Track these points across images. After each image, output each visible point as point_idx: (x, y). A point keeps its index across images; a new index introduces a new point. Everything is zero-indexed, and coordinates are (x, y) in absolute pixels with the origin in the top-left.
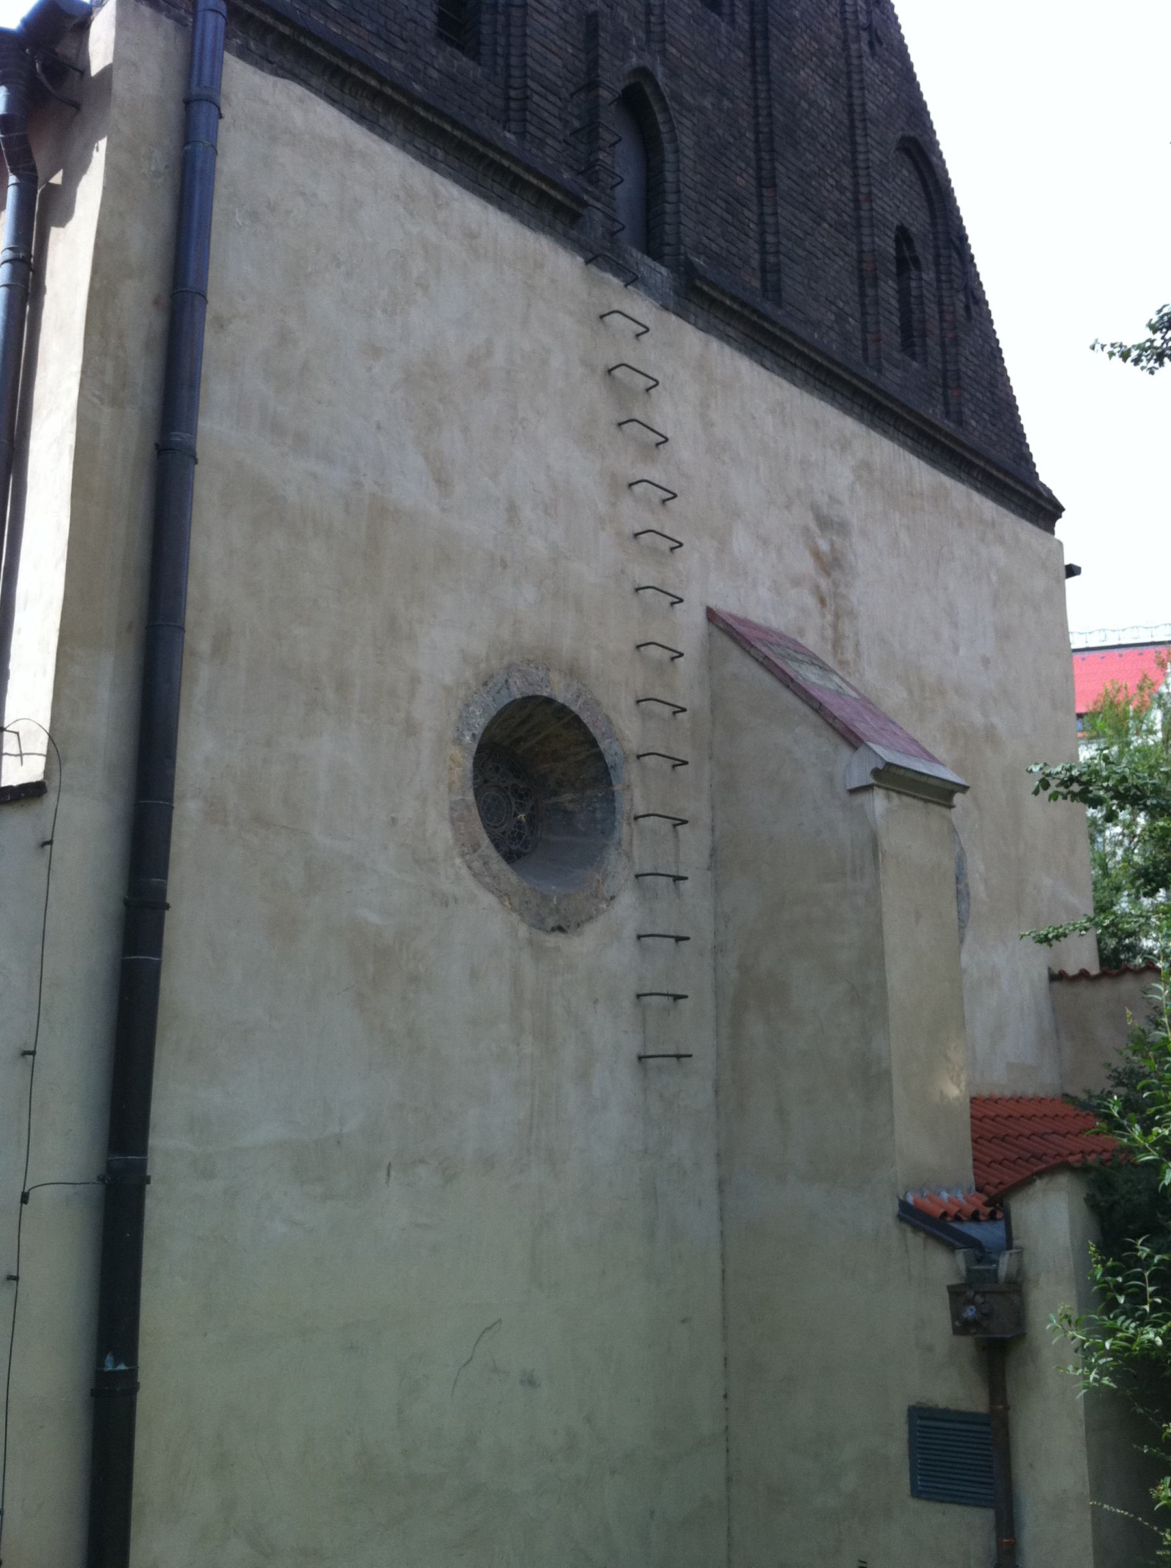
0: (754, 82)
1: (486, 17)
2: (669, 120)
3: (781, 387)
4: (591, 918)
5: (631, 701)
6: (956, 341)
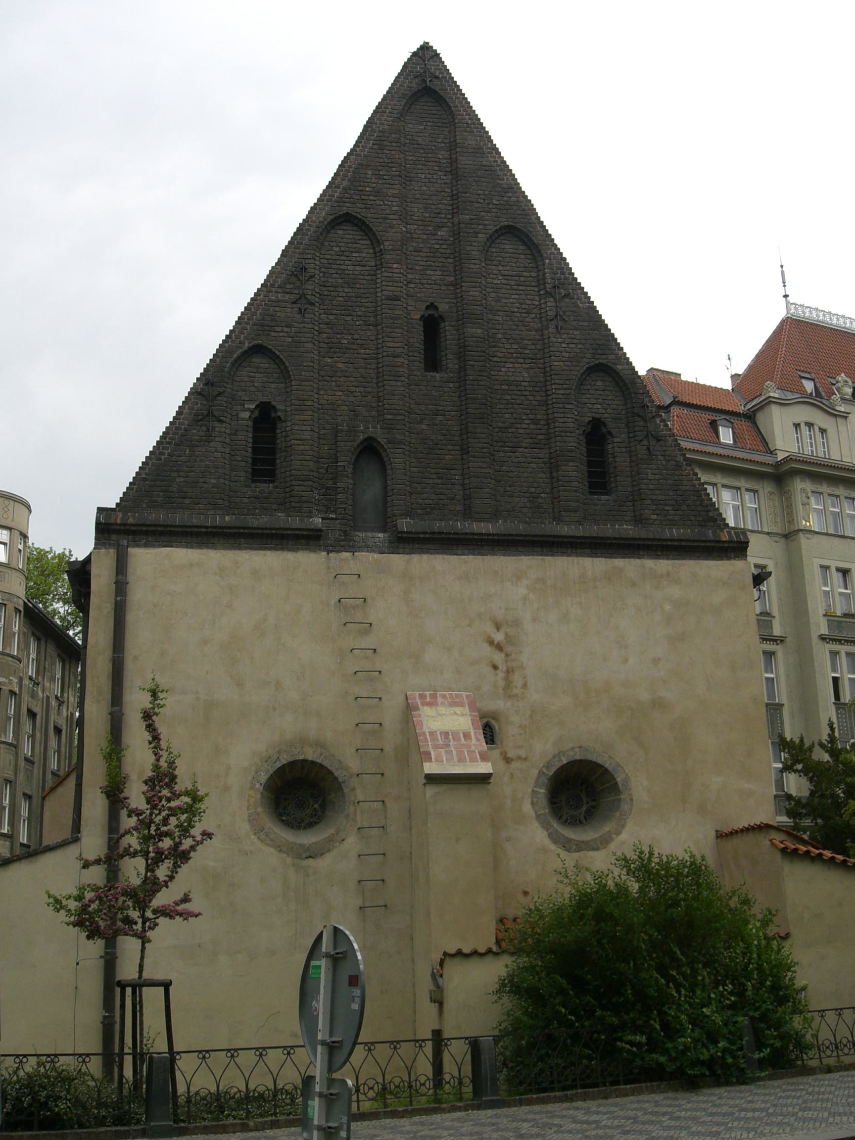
3: (466, 562)
4: (329, 851)
5: (354, 751)
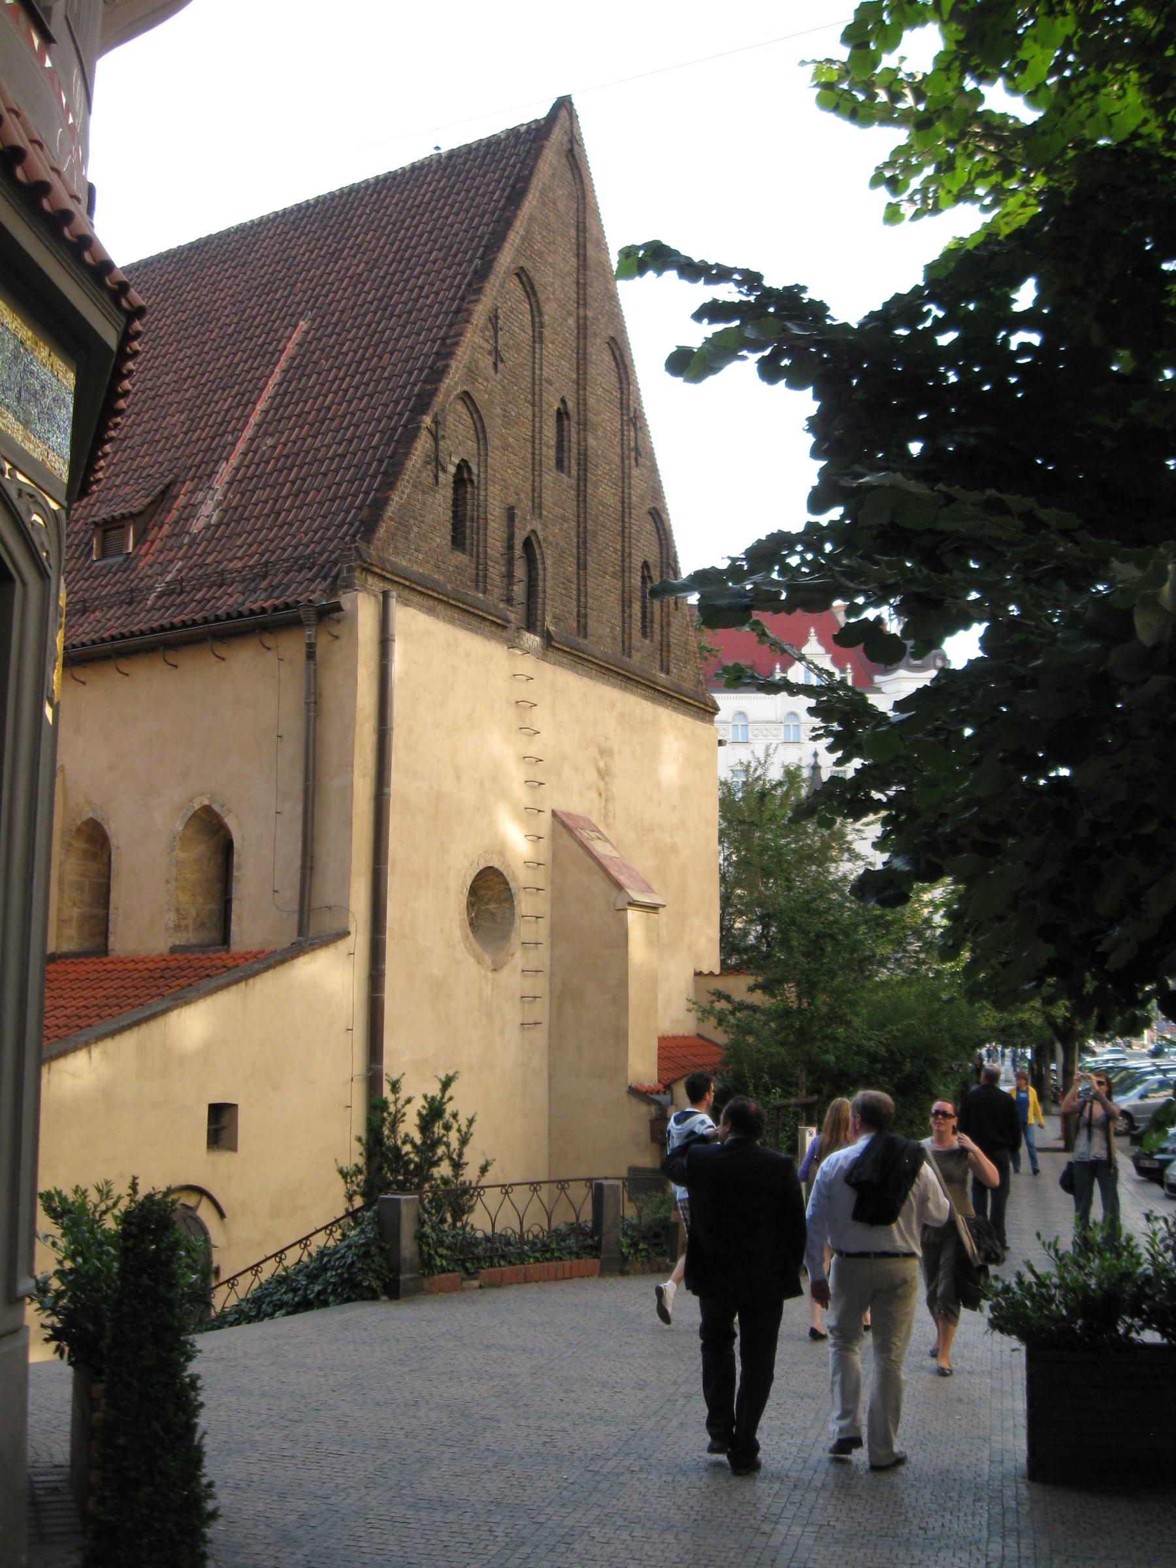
0: (578, 506)
1: (468, 524)
2: (542, 553)
6: (668, 624)
